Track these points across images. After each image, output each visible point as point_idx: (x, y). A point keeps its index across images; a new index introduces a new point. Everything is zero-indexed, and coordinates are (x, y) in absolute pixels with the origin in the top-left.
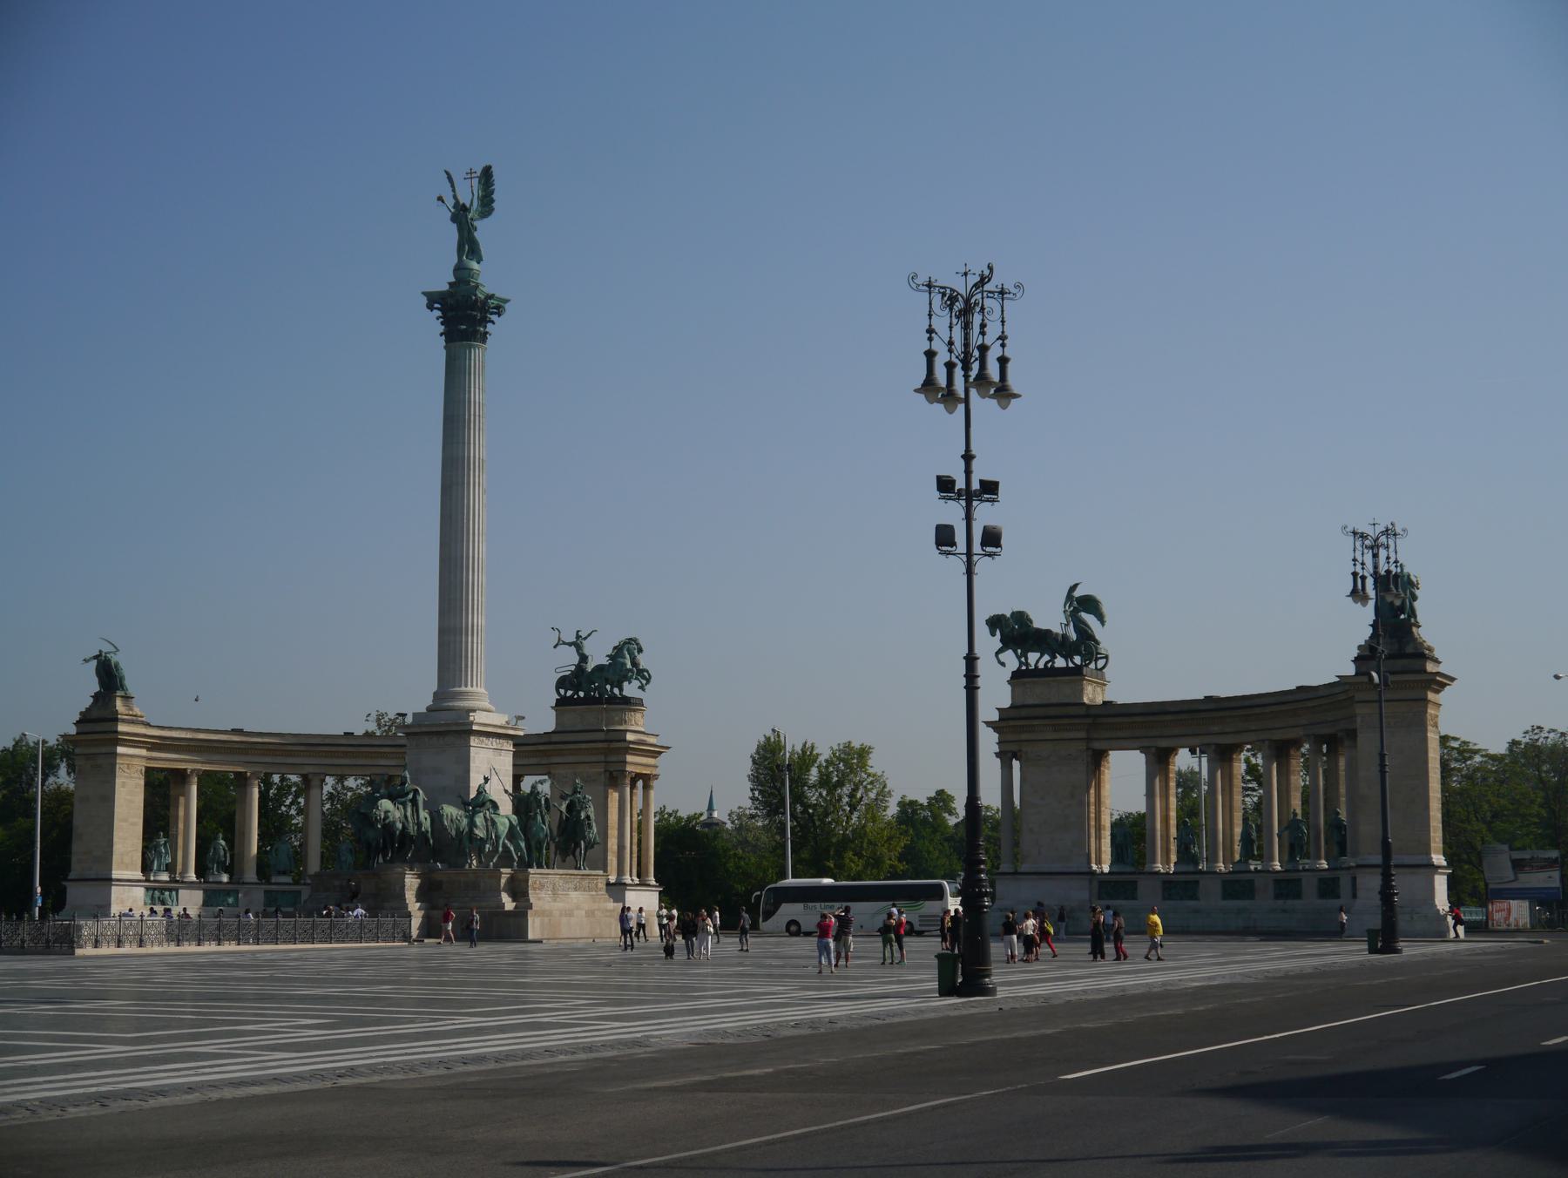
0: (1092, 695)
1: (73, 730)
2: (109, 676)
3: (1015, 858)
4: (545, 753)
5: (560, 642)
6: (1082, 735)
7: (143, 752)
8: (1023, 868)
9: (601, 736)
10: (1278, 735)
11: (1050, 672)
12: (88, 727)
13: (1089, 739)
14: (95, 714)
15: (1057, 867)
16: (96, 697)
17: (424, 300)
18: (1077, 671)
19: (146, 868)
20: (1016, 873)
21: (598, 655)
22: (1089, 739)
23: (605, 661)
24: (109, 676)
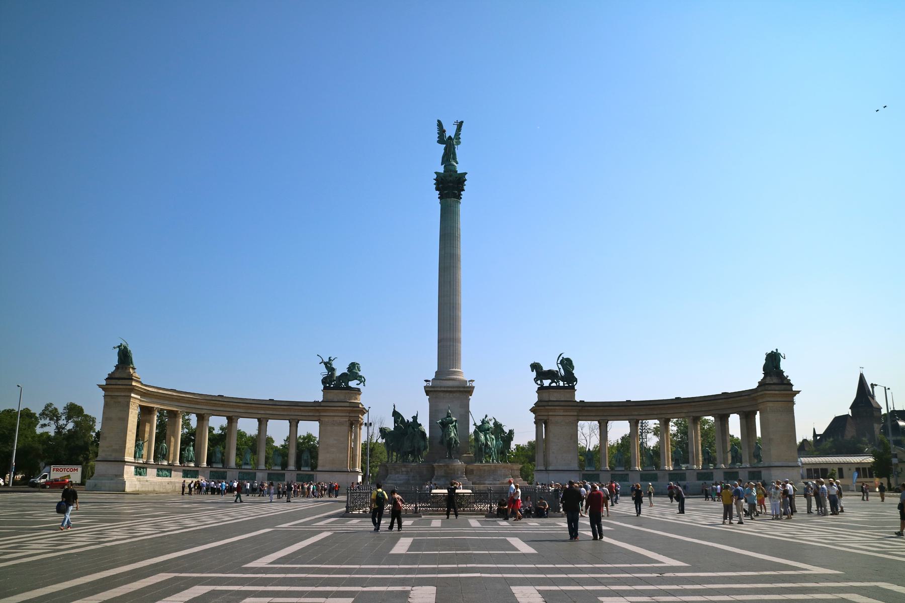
0: (578, 399)
1: (104, 383)
2: (125, 357)
9: (347, 404)
10: (668, 417)
11: (558, 387)
13: (578, 416)
14: (117, 375)
15: (565, 468)
16: (117, 367)
18: (573, 388)
19: (135, 457)
20: (546, 470)
21: (341, 369)
22: (578, 416)
24: (125, 357)
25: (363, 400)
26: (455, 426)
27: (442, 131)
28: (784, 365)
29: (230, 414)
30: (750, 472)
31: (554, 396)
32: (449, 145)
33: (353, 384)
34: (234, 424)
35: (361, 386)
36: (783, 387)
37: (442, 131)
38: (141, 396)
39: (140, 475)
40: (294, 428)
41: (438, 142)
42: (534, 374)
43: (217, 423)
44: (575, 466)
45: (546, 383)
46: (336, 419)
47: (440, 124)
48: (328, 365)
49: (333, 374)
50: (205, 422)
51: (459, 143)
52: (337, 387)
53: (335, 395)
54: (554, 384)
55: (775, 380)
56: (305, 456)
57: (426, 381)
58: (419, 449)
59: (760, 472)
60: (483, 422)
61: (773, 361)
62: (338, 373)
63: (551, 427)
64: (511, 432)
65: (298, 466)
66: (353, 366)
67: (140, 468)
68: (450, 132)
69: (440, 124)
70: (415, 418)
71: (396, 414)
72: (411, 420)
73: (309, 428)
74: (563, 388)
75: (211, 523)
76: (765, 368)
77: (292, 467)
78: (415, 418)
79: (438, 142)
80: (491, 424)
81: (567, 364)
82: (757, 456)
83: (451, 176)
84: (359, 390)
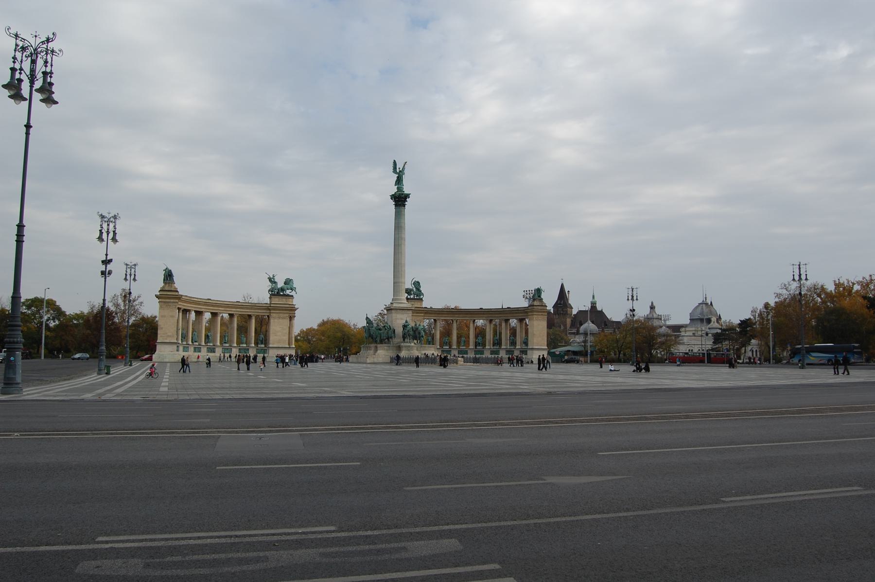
2: (169, 276)
14: (167, 288)
24: (169, 276)
25: (296, 302)
35: (293, 293)
48: (272, 280)
52: (278, 294)
53: (276, 301)
65: (256, 343)
66: (288, 282)
68: (400, 166)
81: (417, 284)
82: (526, 343)
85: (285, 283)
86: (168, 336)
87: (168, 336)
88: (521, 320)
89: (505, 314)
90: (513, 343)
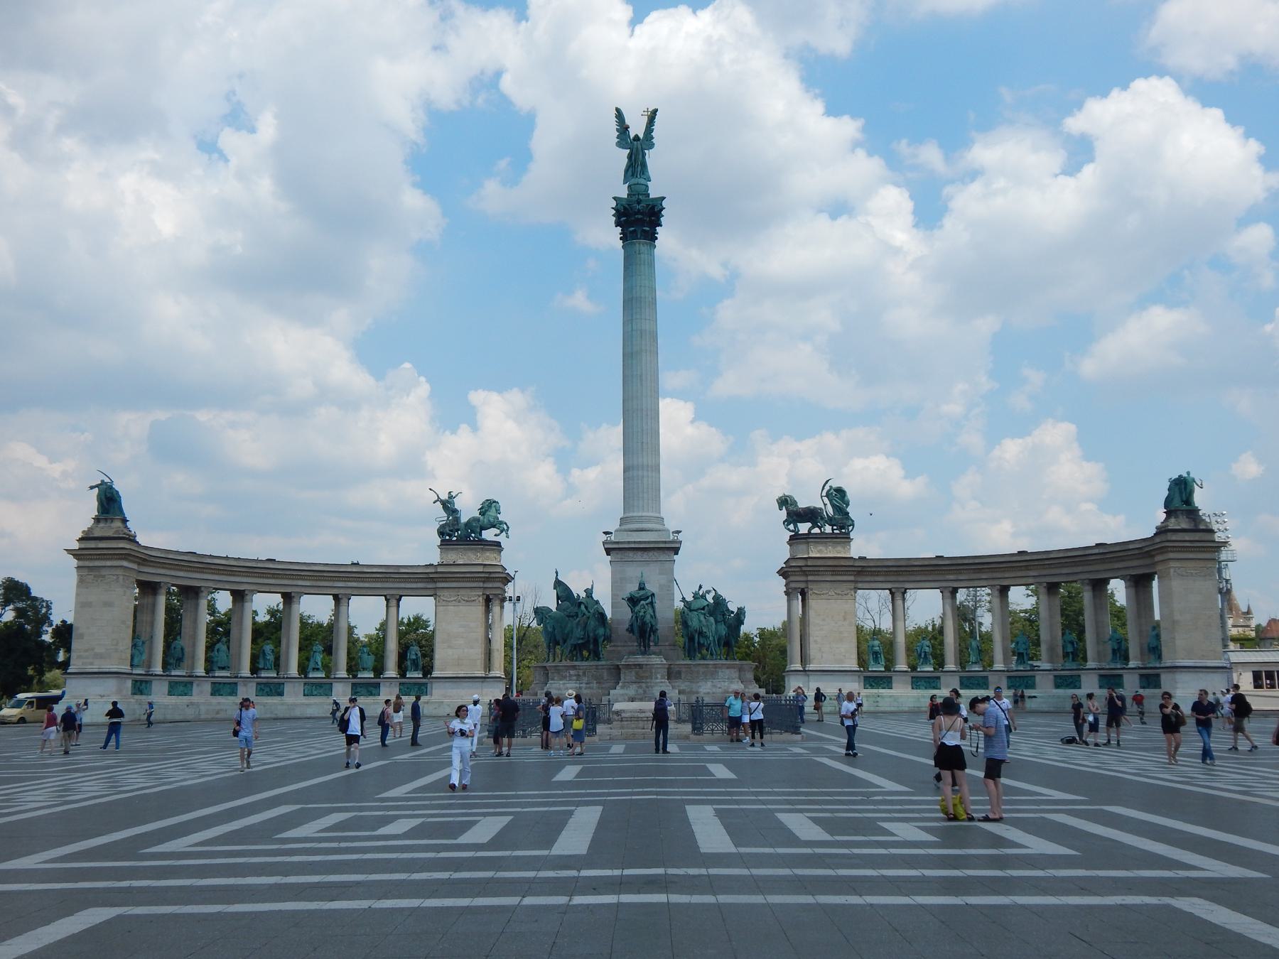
2: (109, 502)
3: (804, 660)
4: (433, 580)
5: (439, 499)
6: (852, 578)
7: (135, 566)
8: (811, 667)
10: (1005, 583)
11: (823, 537)
12: (92, 544)
14: (97, 534)
16: (97, 520)
17: (614, 204)
18: (845, 538)
19: (132, 665)
21: (468, 509)
23: (477, 514)
24: (109, 502)
25: (509, 560)
26: (652, 603)
27: (623, 129)
28: (1200, 499)
29: (288, 590)
30: (1142, 676)
31: (815, 552)
32: (636, 149)
33: (489, 535)
34: (295, 606)
35: (502, 538)
36: (1197, 536)
37: (623, 129)
38: (139, 564)
39: (142, 694)
40: (393, 610)
41: (620, 145)
42: (783, 514)
43: (263, 604)
44: (853, 665)
45: (804, 528)
46: (462, 592)
47: (619, 115)
48: (448, 505)
49: (457, 520)
50: (247, 605)
51: (651, 146)
53: (462, 557)
54: (816, 530)
55: (1184, 524)
56: (415, 651)
57: (606, 533)
58: (596, 641)
59: (1158, 676)
60: (696, 596)
61: (1181, 491)
62: (464, 519)
63: (813, 603)
64: (741, 612)
65: (402, 670)
66: (489, 506)
67: (141, 681)
68: (637, 128)
69: (619, 115)
70: (589, 592)
71: (558, 584)
72: (583, 595)
73: (415, 606)
74: (831, 537)
75: (294, 758)
76: (1168, 503)
77: (391, 672)
78: (589, 592)
79: (620, 145)
80: (710, 598)
82: (1155, 650)
83: (639, 202)
84: (498, 544)
85: (483, 513)
86: (100, 656)
87: (100, 656)
88: (1140, 583)
89: (1094, 564)
90: (1121, 653)
